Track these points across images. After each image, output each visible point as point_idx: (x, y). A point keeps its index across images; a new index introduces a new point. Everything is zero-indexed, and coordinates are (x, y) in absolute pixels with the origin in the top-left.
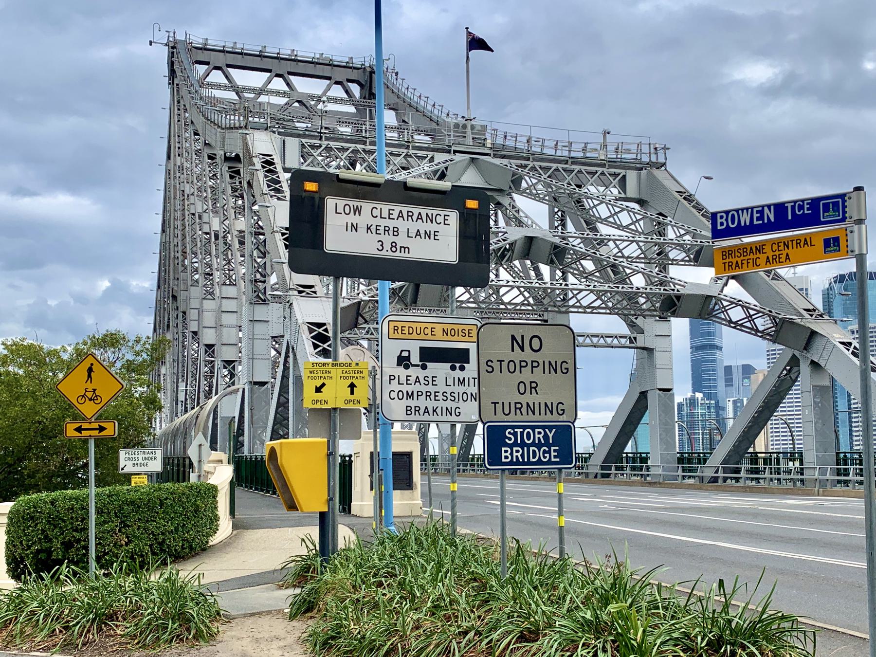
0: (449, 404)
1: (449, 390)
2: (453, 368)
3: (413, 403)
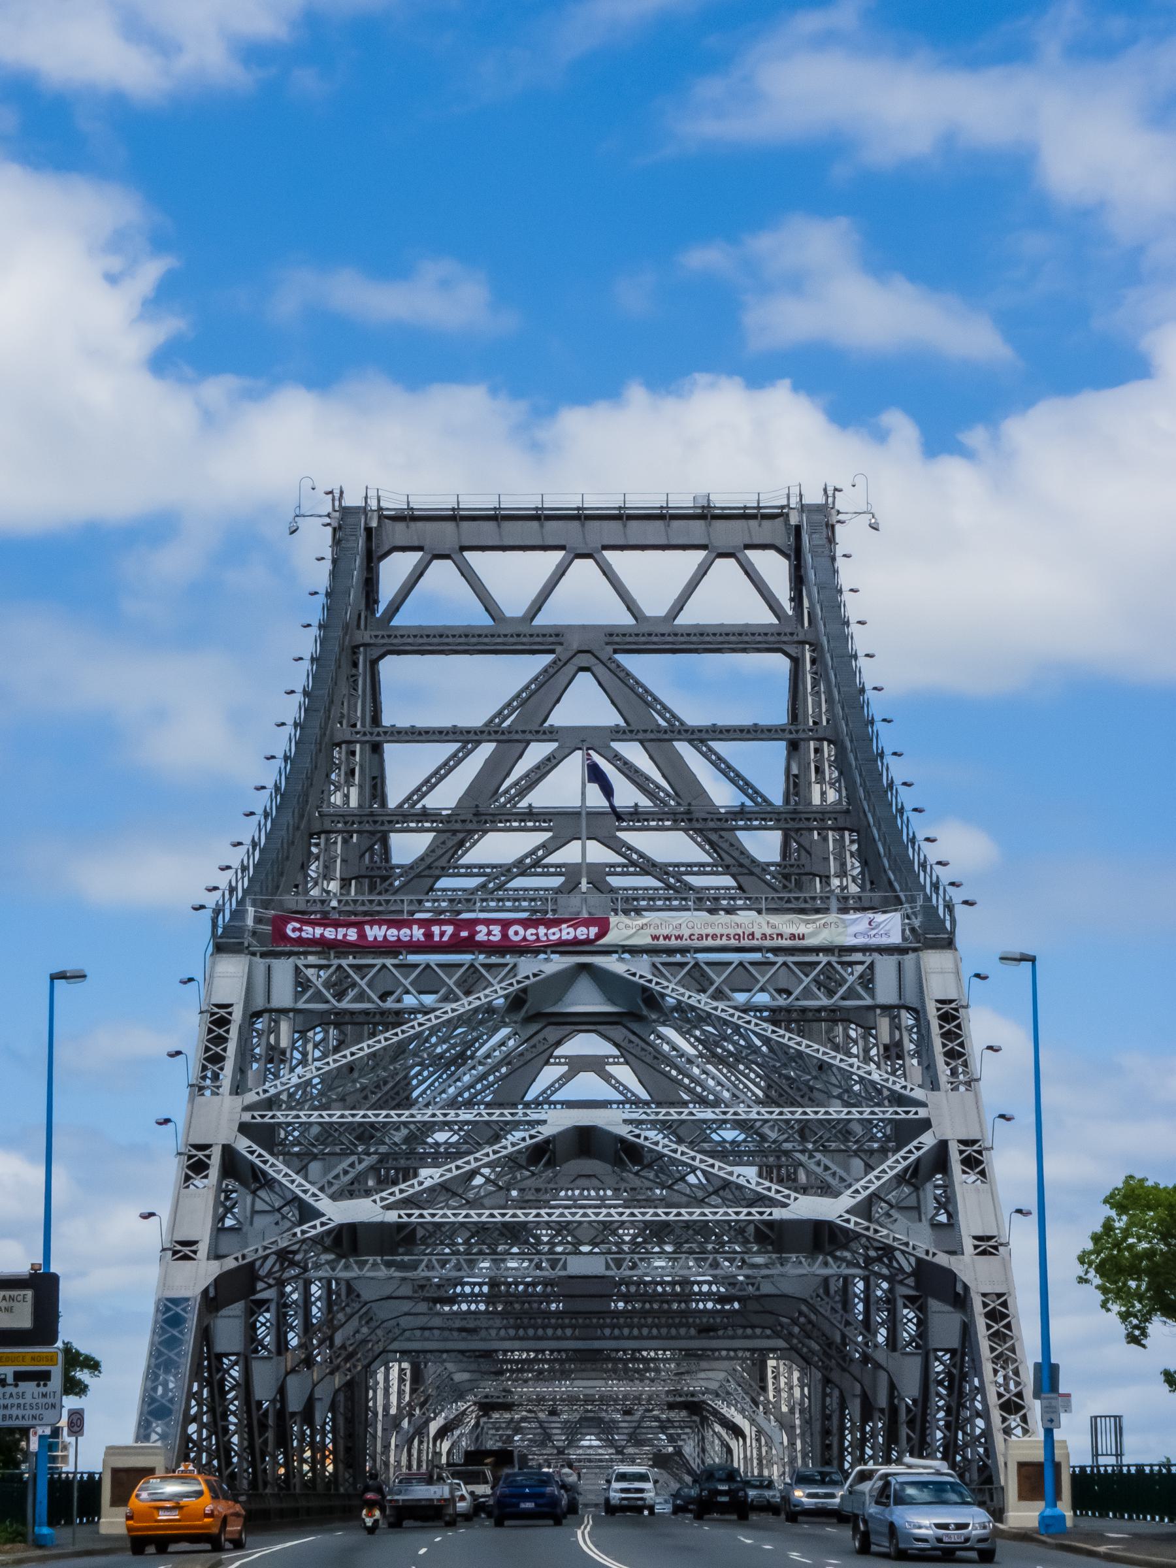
0: (34, 1412)
1: (34, 1402)
2: (38, 1385)
3: (7, 1412)
